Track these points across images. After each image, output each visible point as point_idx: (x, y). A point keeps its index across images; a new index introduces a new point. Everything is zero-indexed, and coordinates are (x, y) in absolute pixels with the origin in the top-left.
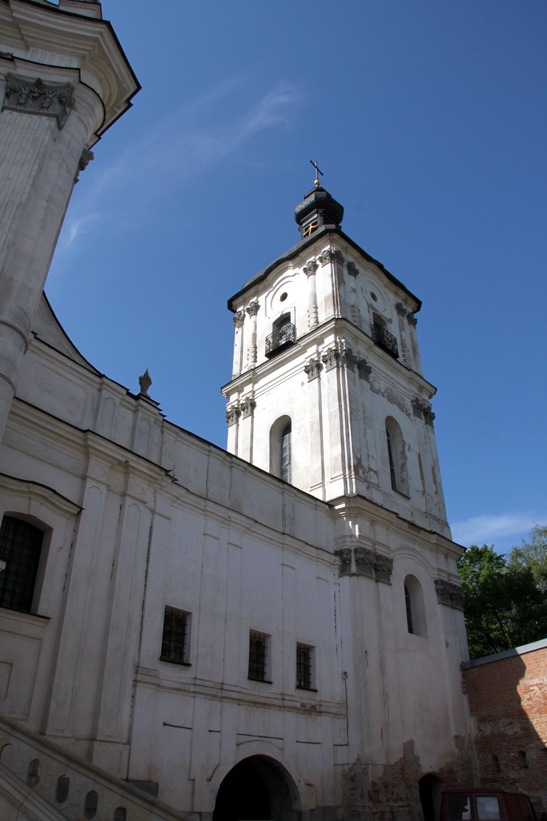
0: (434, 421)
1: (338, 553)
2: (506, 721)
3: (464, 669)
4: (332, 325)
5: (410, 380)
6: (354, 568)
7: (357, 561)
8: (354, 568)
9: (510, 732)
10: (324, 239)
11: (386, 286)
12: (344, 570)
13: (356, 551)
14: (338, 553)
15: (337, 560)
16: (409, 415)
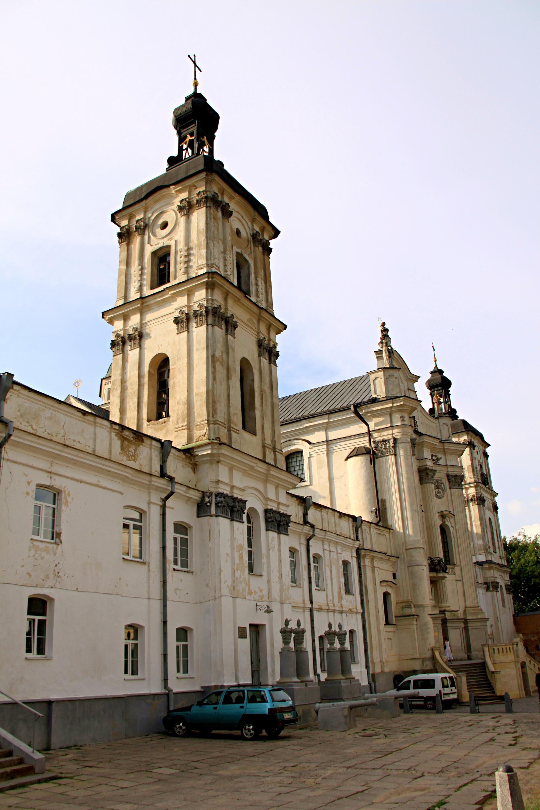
0: (498, 510)
1: (485, 583)
2: (532, 635)
3: (514, 616)
4: (474, 484)
5: (491, 495)
6: (491, 589)
7: (492, 586)
8: (491, 589)
9: (533, 639)
10: (465, 433)
11: (480, 443)
12: (488, 589)
13: (492, 582)
14: (485, 583)
15: (485, 586)
16: (491, 512)
